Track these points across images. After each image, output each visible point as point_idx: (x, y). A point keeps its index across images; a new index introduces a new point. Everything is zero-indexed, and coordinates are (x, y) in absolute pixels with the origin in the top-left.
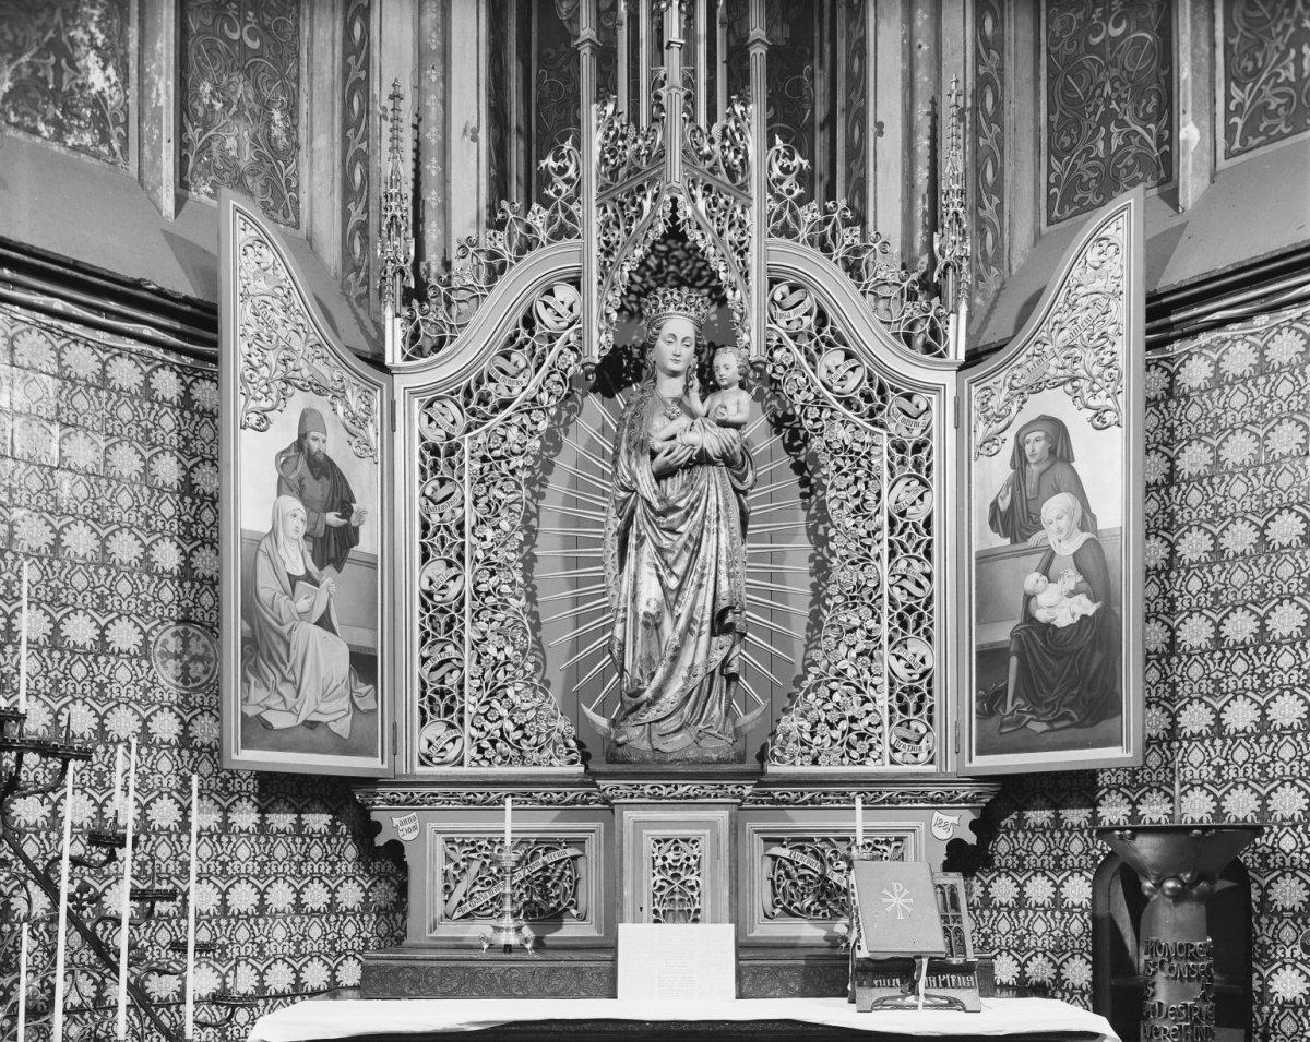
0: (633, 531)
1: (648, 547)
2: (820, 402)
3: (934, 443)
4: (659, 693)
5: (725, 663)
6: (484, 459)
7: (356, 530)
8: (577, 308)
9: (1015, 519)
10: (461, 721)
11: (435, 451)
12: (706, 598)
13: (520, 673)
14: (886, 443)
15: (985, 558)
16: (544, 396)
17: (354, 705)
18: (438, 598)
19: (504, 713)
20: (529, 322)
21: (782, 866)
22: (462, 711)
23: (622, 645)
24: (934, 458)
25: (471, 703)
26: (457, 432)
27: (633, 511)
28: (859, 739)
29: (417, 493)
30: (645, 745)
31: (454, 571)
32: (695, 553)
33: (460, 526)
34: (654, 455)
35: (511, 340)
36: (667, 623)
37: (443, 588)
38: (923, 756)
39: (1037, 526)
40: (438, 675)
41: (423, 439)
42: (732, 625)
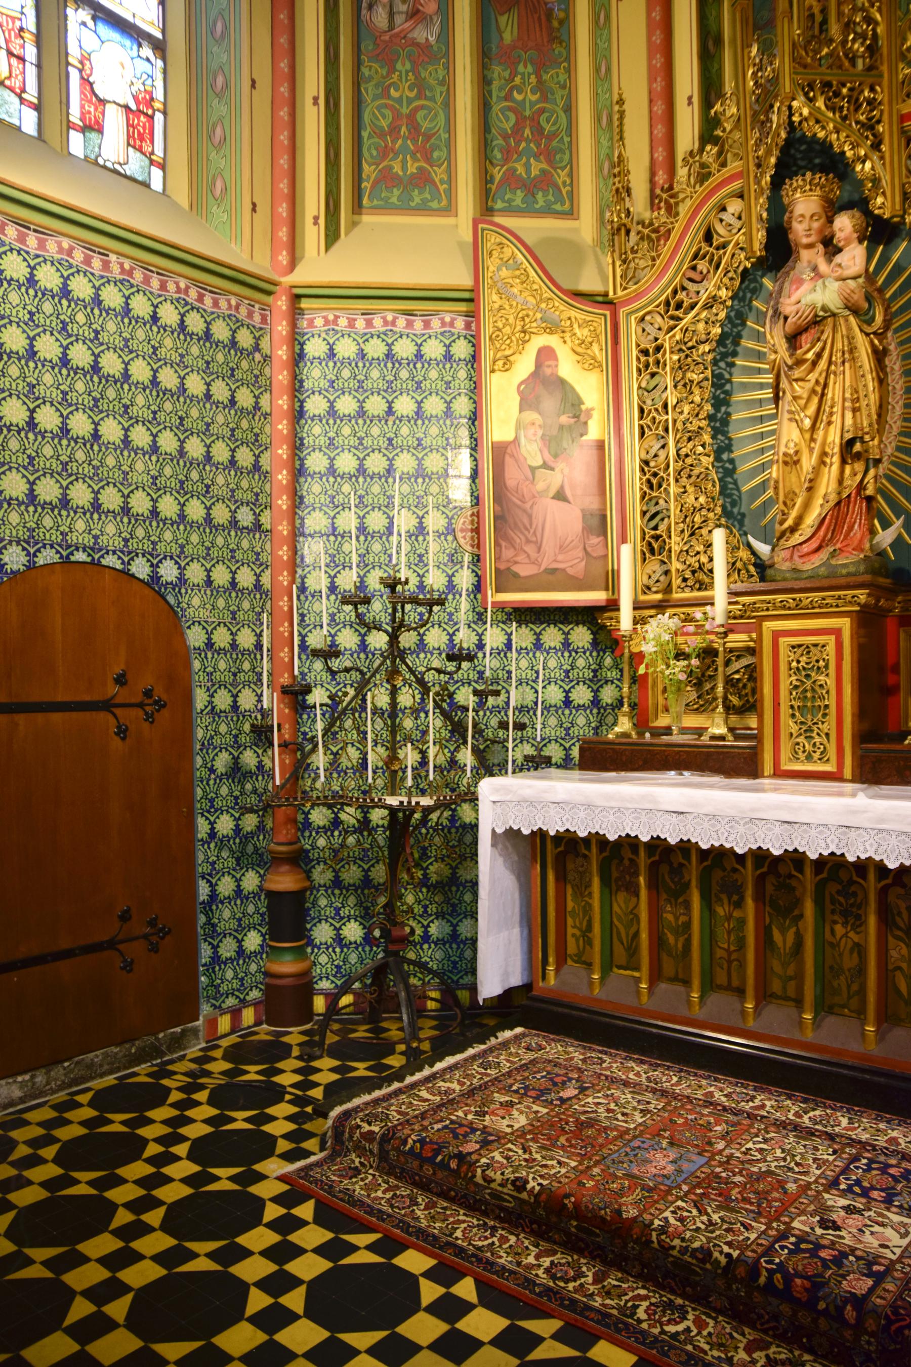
5: (861, 487)
6: (681, 350)
10: (670, 557)
11: (645, 352)
13: (711, 515)
16: (723, 293)
18: (652, 464)
20: (708, 237)
22: (670, 551)
25: (675, 543)
26: (661, 335)
29: (636, 387)
33: (665, 406)
35: (695, 257)
37: (656, 456)
40: (653, 523)
41: (638, 345)
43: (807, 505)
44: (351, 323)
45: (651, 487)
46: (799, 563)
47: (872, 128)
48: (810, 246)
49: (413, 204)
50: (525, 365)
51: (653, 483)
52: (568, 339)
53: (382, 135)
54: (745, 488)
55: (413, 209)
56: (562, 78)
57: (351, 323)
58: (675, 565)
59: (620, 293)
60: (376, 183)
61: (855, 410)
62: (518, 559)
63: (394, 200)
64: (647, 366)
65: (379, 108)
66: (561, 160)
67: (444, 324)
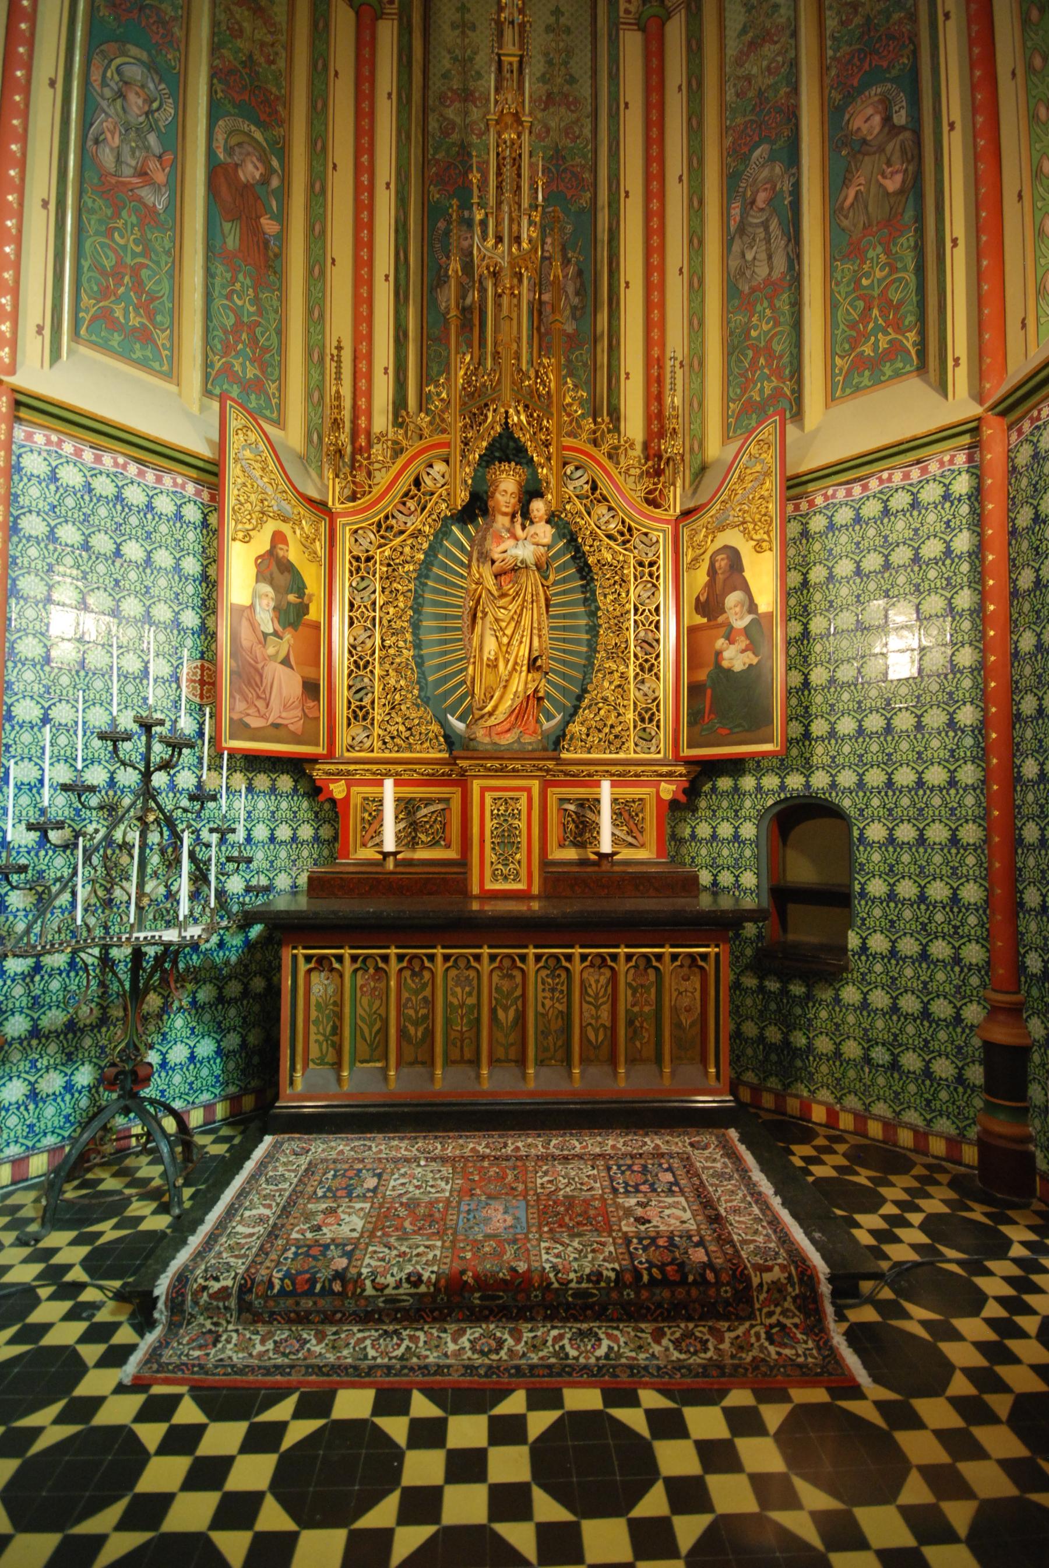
0: (480, 608)
1: (490, 618)
2: (594, 536)
3: (661, 562)
4: (496, 707)
5: (536, 691)
6: (389, 565)
7: (307, 607)
8: (447, 476)
9: (709, 606)
10: (372, 724)
11: (357, 559)
12: (524, 651)
14: (632, 562)
15: (692, 630)
16: (427, 528)
17: (305, 714)
19: (400, 720)
20: (417, 482)
21: (570, 815)
22: (373, 719)
23: (473, 678)
24: (661, 571)
25: (378, 714)
26: (372, 548)
27: (480, 597)
28: (617, 741)
29: (347, 584)
30: (487, 740)
31: (369, 633)
32: (518, 623)
34: (493, 562)
35: (406, 494)
36: (501, 664)
38: (653, 749)
39: (723, 611)
40: (358, 696)
42: (540, 667)
43: (501, 697)
44: (78, 453)
45: (358, 667)
46: (496, 739)
47: (547, 447)
48: (505, 514)
49: (134, 357)
50: (262, 543)
51: (360, 664)
52: (298, 532)
53: (103, 272)
54: (430, 679)
55: (134, 361)
56: (276, 303)
57: (78, 453)
58: (377, 731)
59: (337, 505)
60: (93, 319)
61: (540, 637)
62: (249, 711)
63: (115, 344)
64: (358, 570)
65: (103, 245)
66: (272, 374)
67: (175, 484)
